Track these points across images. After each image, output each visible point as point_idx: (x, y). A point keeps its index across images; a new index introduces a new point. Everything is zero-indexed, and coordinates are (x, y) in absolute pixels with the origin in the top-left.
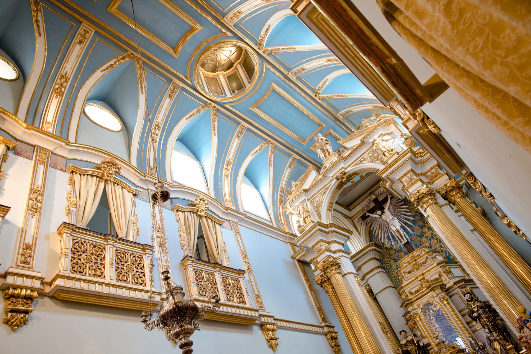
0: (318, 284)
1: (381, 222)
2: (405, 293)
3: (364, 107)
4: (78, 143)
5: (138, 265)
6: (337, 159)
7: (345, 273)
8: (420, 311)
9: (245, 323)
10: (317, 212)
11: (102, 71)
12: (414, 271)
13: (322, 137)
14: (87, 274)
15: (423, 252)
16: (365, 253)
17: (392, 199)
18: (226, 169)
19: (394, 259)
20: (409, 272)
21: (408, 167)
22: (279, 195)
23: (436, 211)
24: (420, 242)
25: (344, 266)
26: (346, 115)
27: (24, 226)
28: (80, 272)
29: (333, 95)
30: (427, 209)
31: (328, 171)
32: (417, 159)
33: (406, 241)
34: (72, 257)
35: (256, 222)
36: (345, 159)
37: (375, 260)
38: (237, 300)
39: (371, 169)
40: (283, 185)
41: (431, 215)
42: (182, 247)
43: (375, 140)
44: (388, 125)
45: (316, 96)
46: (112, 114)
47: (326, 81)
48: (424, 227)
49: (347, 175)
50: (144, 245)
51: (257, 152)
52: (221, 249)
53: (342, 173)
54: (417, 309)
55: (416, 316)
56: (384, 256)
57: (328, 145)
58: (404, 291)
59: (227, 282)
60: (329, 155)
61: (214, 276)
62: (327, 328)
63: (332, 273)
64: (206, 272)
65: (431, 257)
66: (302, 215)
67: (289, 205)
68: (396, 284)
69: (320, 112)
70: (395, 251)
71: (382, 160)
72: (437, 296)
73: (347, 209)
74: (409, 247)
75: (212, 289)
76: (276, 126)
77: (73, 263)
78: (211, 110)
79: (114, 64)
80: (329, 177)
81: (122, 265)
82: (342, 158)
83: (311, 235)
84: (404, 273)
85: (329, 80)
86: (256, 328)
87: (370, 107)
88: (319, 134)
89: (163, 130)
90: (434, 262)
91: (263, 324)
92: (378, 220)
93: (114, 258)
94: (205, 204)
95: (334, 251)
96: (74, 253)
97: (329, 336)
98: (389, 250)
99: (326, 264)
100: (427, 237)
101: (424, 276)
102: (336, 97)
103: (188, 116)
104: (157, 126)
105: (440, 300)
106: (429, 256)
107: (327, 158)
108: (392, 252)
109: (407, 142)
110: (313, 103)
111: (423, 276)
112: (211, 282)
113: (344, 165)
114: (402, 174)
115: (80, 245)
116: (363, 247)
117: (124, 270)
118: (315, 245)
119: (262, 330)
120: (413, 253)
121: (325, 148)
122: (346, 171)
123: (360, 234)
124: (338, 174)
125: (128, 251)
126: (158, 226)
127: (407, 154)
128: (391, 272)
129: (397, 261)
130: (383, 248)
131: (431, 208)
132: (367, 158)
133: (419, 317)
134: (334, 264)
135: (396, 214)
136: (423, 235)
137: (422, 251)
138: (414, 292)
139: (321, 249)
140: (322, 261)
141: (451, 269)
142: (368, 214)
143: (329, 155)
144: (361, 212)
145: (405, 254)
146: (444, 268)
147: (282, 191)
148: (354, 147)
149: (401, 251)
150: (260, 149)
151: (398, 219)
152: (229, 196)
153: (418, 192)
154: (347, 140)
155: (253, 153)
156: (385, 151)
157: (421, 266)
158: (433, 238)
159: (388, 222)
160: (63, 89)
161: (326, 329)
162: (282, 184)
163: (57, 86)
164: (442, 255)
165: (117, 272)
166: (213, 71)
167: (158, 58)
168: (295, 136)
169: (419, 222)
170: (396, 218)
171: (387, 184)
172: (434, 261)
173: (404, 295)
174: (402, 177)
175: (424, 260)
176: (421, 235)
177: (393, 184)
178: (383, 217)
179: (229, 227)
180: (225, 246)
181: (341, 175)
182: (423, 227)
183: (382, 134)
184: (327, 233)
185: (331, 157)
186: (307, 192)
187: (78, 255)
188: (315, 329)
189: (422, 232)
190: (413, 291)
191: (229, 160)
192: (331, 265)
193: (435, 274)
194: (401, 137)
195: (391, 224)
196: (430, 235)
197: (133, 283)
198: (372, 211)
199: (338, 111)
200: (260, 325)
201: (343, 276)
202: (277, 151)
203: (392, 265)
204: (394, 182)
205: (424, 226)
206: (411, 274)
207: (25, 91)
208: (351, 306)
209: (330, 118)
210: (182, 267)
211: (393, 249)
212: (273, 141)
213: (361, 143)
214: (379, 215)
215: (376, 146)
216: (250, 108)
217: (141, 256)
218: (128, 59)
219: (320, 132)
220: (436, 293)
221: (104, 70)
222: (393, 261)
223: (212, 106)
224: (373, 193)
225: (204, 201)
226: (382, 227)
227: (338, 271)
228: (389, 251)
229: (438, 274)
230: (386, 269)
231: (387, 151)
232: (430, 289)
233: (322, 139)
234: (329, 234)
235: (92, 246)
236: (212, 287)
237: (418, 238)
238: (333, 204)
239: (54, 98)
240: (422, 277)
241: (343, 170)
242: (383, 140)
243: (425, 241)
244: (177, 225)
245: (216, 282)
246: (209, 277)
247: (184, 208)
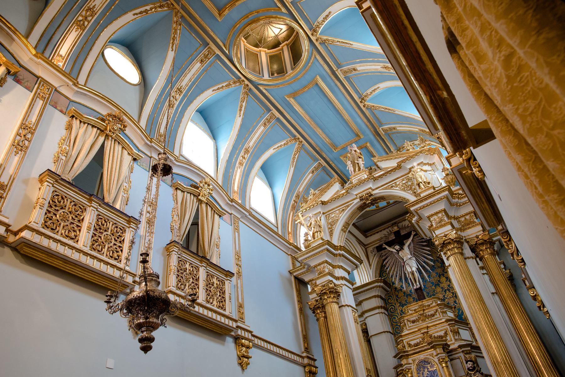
0: (311, 309)
1: (397, 259)
2: (403, 343)
3: (410, 127)
4: (87, 86)
5: (118, 238)
6: (366, 177)
7: (343, 304)
8: (414, 367)
9: (217, 330)
10: (330, 230)
11: (134, 15)
12: (418, 321)
13: (356, 149)
14: (60, 233)
15: (434, 303)
16: (371, 288)
17: (416, 237)
18: (242, 156)
19: (400, 303)
20: (413, 322)
21: (442, 206)
22: (293, 200)
23: (460, 262)
24: (434, 291)
25: (343, 296)
26: (389, 132)
27: (4, 162)
28: (52, 229)
29: (380, 106)
30: (450, 258)
31: (353, 188)
32: (453, 200)
33: (419, 286)
34: (47, 210)
35: (260, 223)
36: (375, 179)
37: (379, 299)
38: (217, 303)
39: (400, 197)
40: (301, 190)
41: (453, 265)
42: (172, 230)
43: (413, 167)
44: (431, 155)
45: (361, 102)
46: (133, 64)
47: (376, 89)
48: (442, 276)
49: (373, 197)
50: (130, 217)
51: (281, 146)
52: (214, 244)
53: (368, 194)
54: (411, 364)
55: (408, 372)
56: (391, 296)
57: (361, 159)
58: (402, 340)
59: (211, 281)
60: (359, 171)
61: (199, 271)
62: (308, 360)
63: (328, 301)
64: (191, 264)
65: (441, 310)
66: (312, 228)
67: (301, 214)
68: (395, 330)
69: (361, 121)
71: (415, 191)
72: (436, 355)
73: (363, 235)
74: (420, 294)
75: (193, 285)
76: (309, 123)
77: (47, 218)
78: (243, 88)
79: (149, 10)
80: (353, 194)
81: (100, 232)
82: (372, 178)
83: (316, 253)
84: (408, 321)
85: (380, 88)
86: (230, 341)
87: (417, 130)
88: (354, 144)
89: (185, 96)
90: (444, 318)
91: (239, 337)
92: (394, 255)
93: (94, 223)
94: (209, 189)
95: (338, 277)
96: (51, 207)
97: (307, 369)
98: (398, 291)
99: (325, 289)
100: (442, 288)
101: (429, 330)
102: (383, 109)
103: (216, 88)
104: (179, 90)
105: (439, 360)
106: (439, 310)
107: (356, 173)
108: (401, 294)
109: (447, 179)
110: (356, 109)
111: (427, 329)
112: (193, 277)
113: (373, 186)
114: (433, 212)
115: (60, 199)
116: (370, 281)
117: (101, 239)
118: (318, 265)
119: (236, 343)
120: (422, 302)
121: (356, 162)
122: (373, 193)
123: (370, 265)
124: (364, 194)
125: (110, 219)
126: (151, 200)
127: (444, 191)
128: (394, 316)
129: (403, 306)
130: (392, 287)
131: (455, 258)
132: (399, 184)
133: (412, 373)
134: (333, 291)
135: (415, 254)
136: (439, 285)
137: (433, 302)
138: (413, 344)
139: (324, 271)
140: (321, 285)
141: (459, 330)
142: (385, 246)
143: (359, 171)
144: (378, 242)
145: (414, 301)
146: (452, 326)
147: (298, 197)
148: (388, 168)
149: (410, 295)
150: (285, 144)
151: (417, 260)
152: (238, 187)
153: (446, 236)
154: (382, 159)
155: (276, 146)
156: (421, 182)
157: (428, 318)
158: (449, 290)
159: (405, 260)
160: (86, 23)
161: (306, 361)
162: (299, 189)
163: (80, 18)
164: (453, 311)
165: (93, 239)
166: (256, 46)
167: (200, 17)
168: (327, 140)
169: (439, 269)
170: (414, 259)
171: (414, 219)
172: (443, 316)
173: (401, 345)
174: (432, 215)
175: (432, 312)
176: (437, 283)
177: (420, 220)
178: (400, 253)
179: (229, 221)
180: (219, 241)
181: (367, 195)
182: (442, 276)
183: (422, 163)
184: (335, 255)
186: (325, 205)
187: (55, 210)
188: (294, 357)
189: (439, 281)
190: (412, 343)
191: (248, 148)
192: (330, 292)
193: (441, 331)
194: (443, 171)
195: (407, 264)
196: (446, 287)
197: (107, 255)
198: (390, 244)
199: (381, 124)
200: (235, 338)
201: (340, 307)
202: (303, 152)
203: (397, 309)
204: (422, 218)
205: (443, 275)
206: (415, 324)
207: (44, 14)
208: (340, 343)
209: (371, 131)
210: (166, 252)
211: (402, 292)
212: (301, 139)
213: (397, 166)
214: (397, 250)
215: (413, 175)
216: (286, 97)
217: (123, 228)
218: (166, 9)
219: (356, 142)
221: (137, 14)
222: (399, 304)
223: (244, 84)
224: (396, 224)
225: (209, 185)
226: (397, 264)
227: (335, 300)
228: (397, 293)
229: (443, 332)
230: (389, 312)
231: (423, 183)
232: (431, 345)
233: (355, 151)
234: (336, 256)
235: (73, 204)
236: (193, 282)
237: (433, 286)
238: (349, 225)
239: (74, 30)
240: (426, 330)
241: (370, 190)
242: (422, 170)
243: (439, 292)
244: (172, 204)
245: (199, 277)
246: (193, 270)
247: (185, 188)
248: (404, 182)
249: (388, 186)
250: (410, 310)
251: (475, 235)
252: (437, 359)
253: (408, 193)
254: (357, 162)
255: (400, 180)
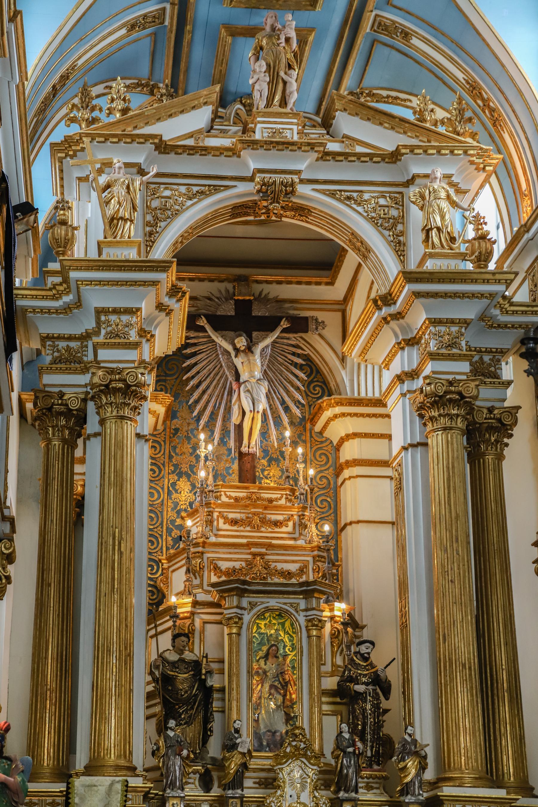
19: (176, 466)
20: (234, 522)
70: (191, 451)
71: (401, 238)
72: (306, 610)
121: (282, 74)
129: (180, 475)
136: (277, 460)
143: (280, 106)
175: (280, 518)
176: (275, 456)
185: (286, 115)
203: (163, 477)
220: (307, 603)
222: (172, 468)
233: (288, 40)
237: (264, 458)
240: (264, 550)
241: (296, 178)
243: (274, 476)
248: (382, 201)
249: (340, 191)
250: (225, 494)
251: (489, 404)
252: (305, 618)
253: (383, 235)
254: (285, 77)
255: (374, 192)
